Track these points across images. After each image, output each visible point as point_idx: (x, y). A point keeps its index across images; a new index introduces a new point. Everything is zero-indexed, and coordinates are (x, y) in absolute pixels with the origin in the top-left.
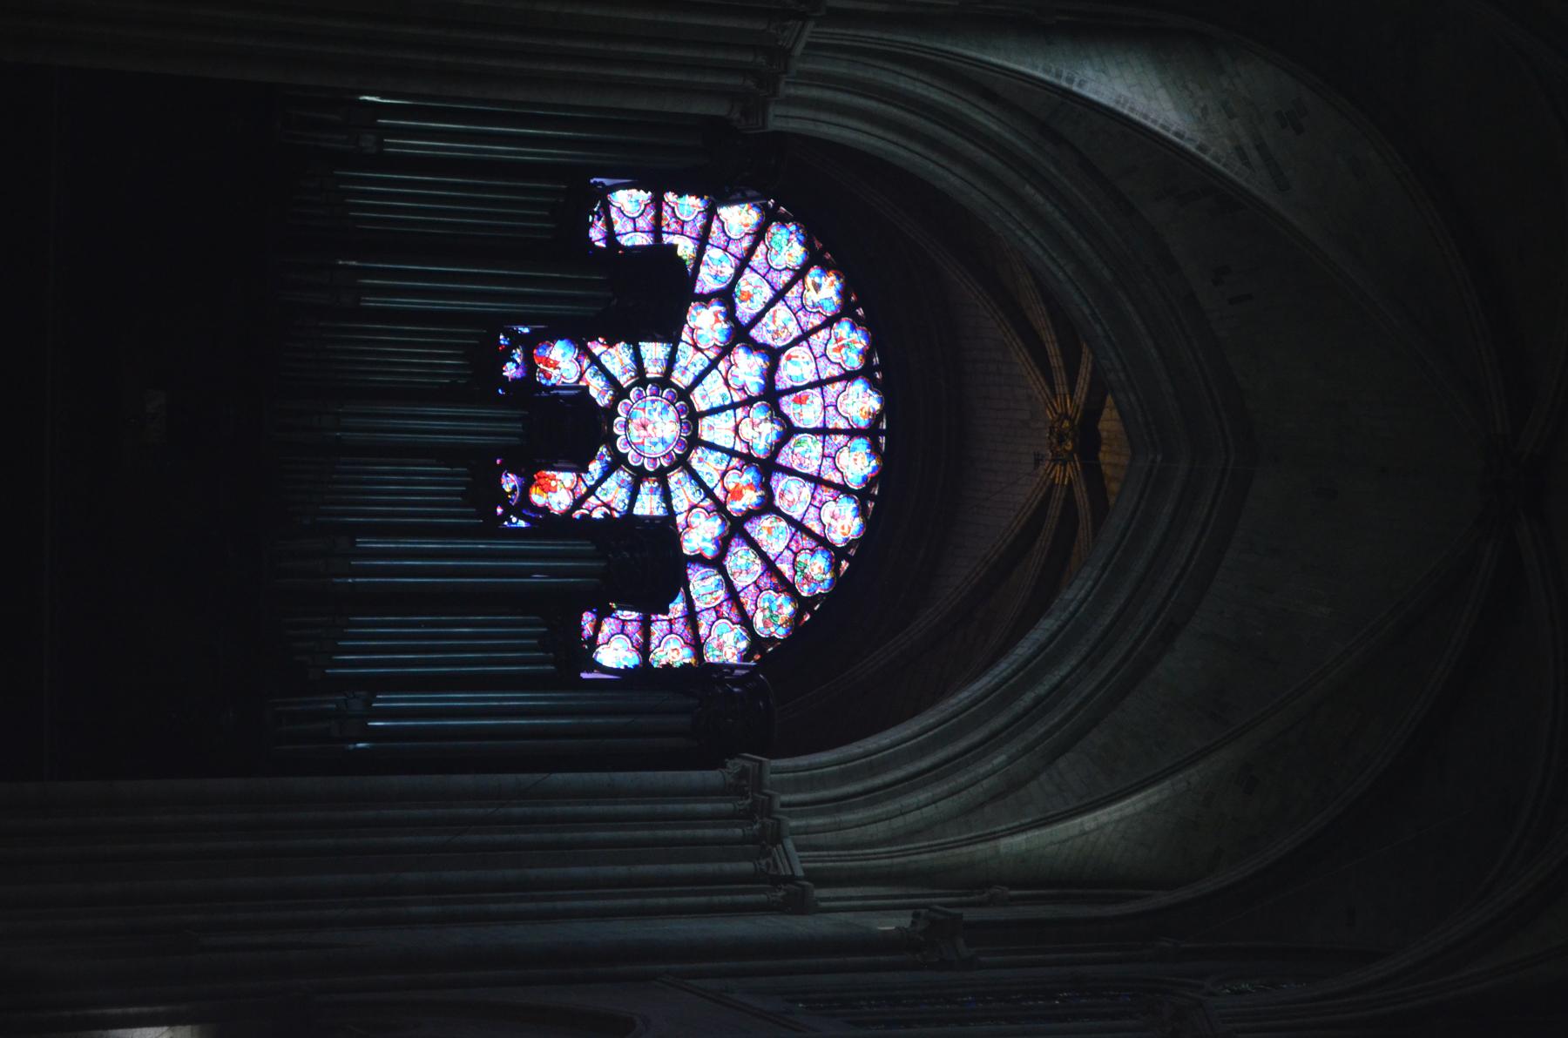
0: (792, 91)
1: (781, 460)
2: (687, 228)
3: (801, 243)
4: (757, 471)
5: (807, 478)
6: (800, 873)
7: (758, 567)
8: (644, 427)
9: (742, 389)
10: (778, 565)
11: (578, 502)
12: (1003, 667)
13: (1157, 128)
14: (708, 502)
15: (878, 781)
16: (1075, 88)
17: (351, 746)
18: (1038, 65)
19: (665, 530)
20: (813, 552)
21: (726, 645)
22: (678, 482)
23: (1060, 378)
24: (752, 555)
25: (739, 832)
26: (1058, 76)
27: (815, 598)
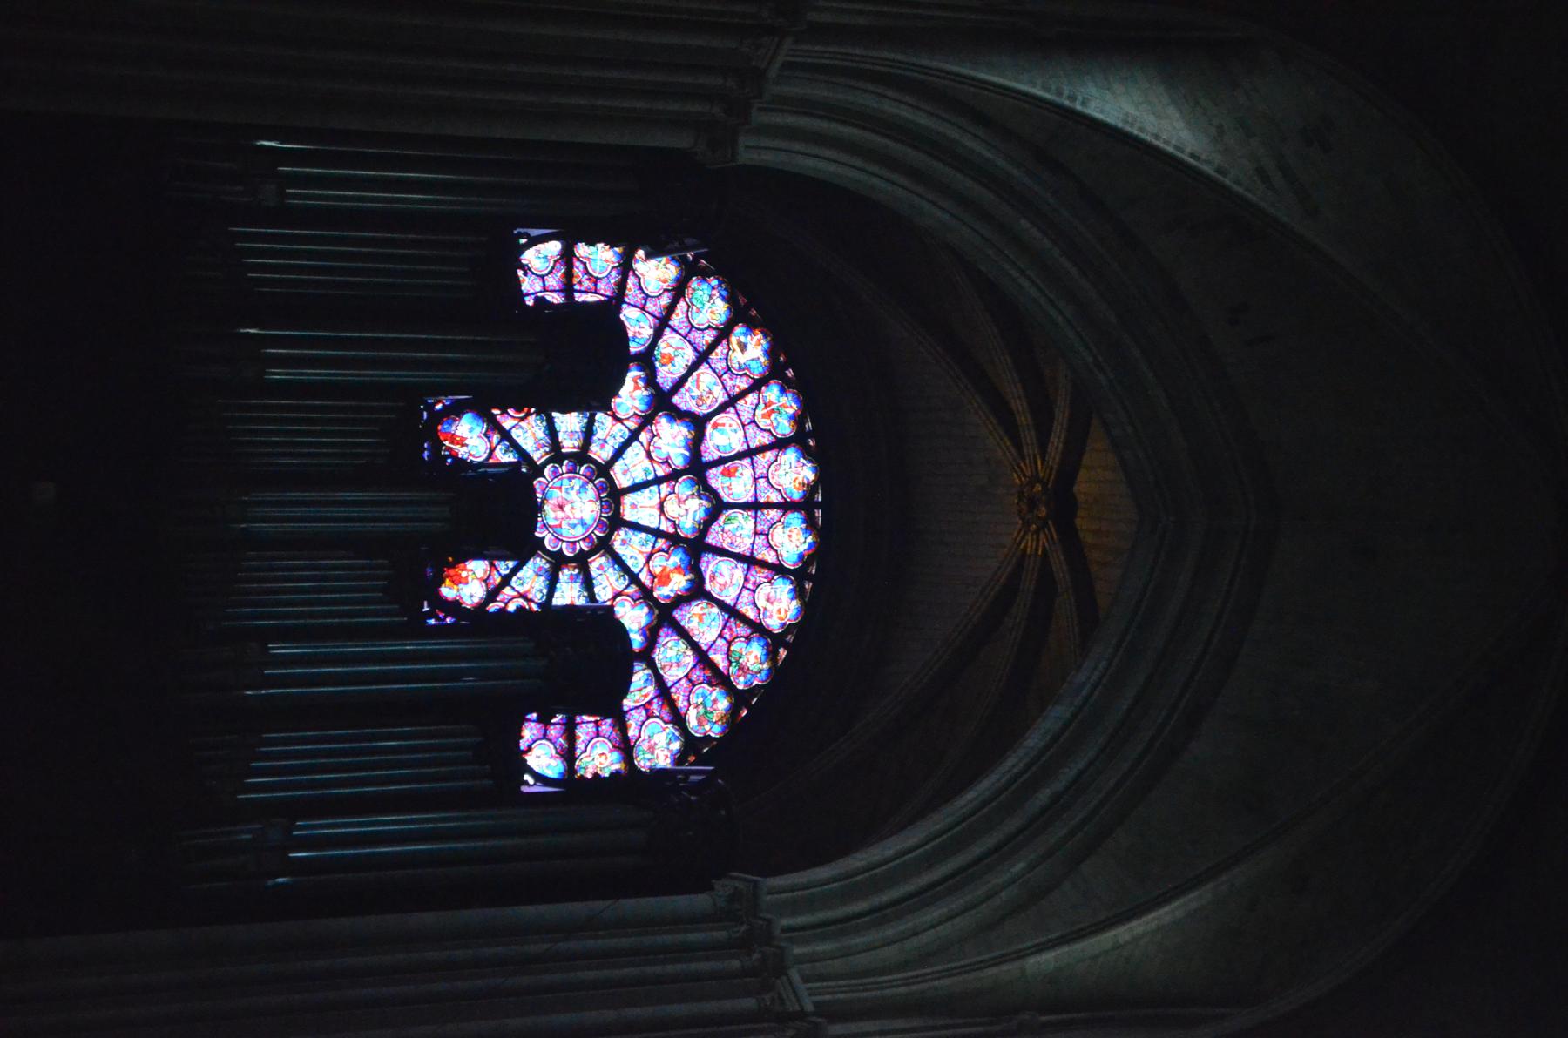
0: (765, 118)
1: (710, 539)
2: (600, 286)
3: (724, 299)
4: (685, 551)
5: (739, 558)
6: (809, 1007)
7: (689, 659)
8: (561, 507)
9: (666, 462)
10: (711, 655)
11: (492, 595)
12: (1012, 763)
13: (1170, 149)
14: (633, 589)
15: (885, 897)
16: (1079, 107)
17: (270, 883)
18: (1036, 84)
19: (601, 619)
20: (748, 640)
21: (658, 747)
22: (601, 567)
23: (1029, 437)
24: (682, 645)
25: (736, 964)
26: (1060, 94)
27: (752, 691)
